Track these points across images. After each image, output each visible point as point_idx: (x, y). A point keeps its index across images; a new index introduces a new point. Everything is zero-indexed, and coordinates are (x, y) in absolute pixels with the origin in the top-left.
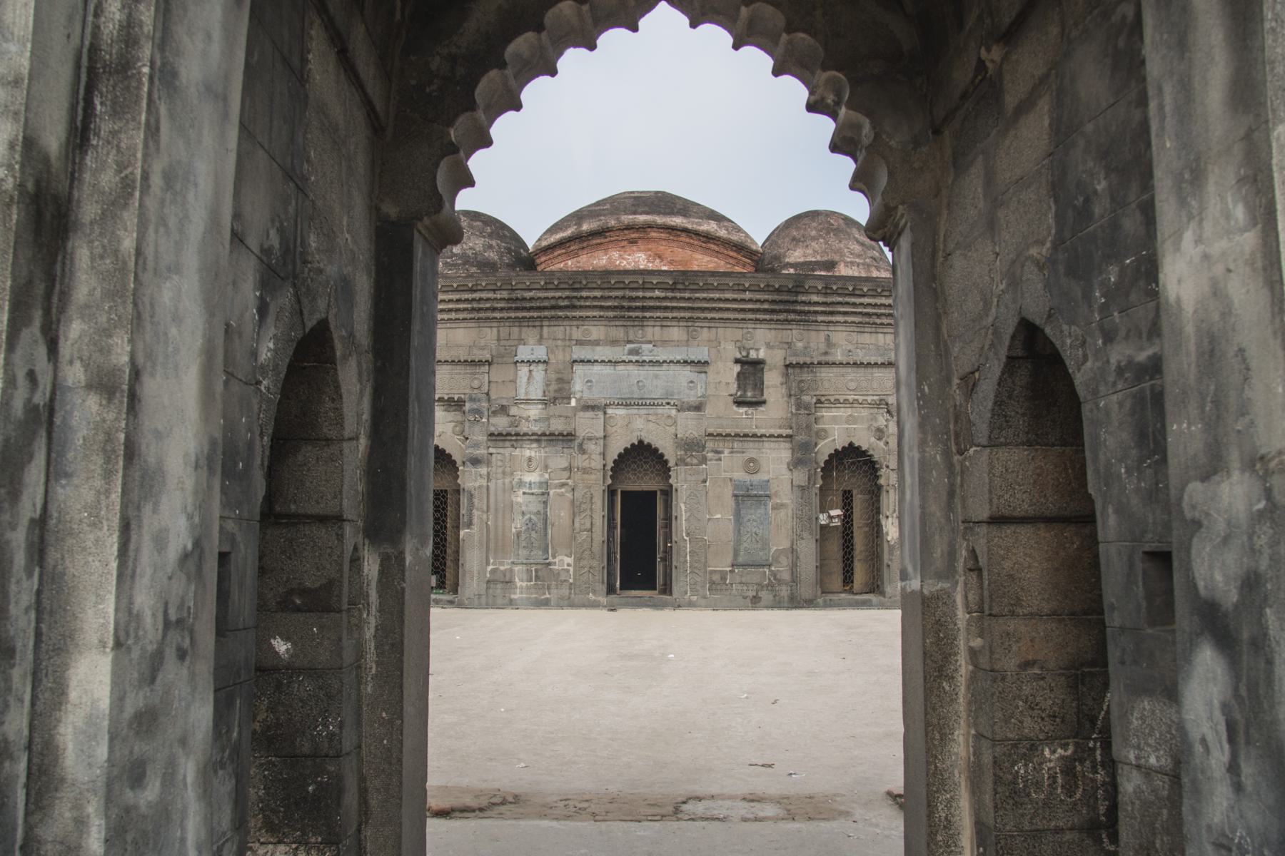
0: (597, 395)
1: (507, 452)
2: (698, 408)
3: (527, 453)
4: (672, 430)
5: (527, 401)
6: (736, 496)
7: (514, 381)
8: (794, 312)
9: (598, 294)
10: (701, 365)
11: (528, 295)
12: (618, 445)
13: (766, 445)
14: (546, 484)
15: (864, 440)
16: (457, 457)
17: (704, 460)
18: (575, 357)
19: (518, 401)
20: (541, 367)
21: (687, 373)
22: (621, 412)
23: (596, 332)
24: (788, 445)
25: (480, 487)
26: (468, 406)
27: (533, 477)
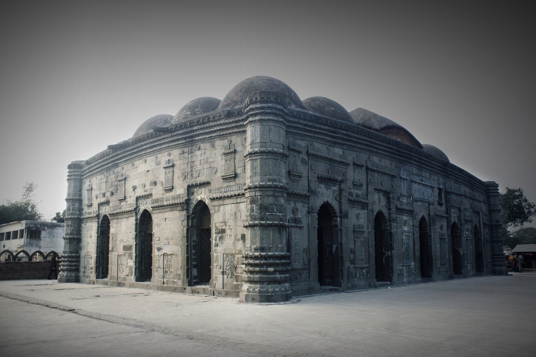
0: (417, 195)
1: (400, 216)
2: (433, 205)
3: (405, 218)
4: (427, 212)
5: (404, 196)
6: (440, 238)
7: (401, 186)
8: (447, 173)
9: (415, 155)
10: (432, 187)
11: (402, 150)
12: (420, 217)
13: (444, 220)
14: (408, 232)
15: (456, 221)
16: (387, 218)
17: (435, 224)
18: (413, 180)
19: (402, 195)
20: (405, 182)
21: (429, 191)
22: (419, 203)
23: (415, 171)
24: (446, 220)
25: (395, 232)
26: (391, 196)
27: (406, 229)
